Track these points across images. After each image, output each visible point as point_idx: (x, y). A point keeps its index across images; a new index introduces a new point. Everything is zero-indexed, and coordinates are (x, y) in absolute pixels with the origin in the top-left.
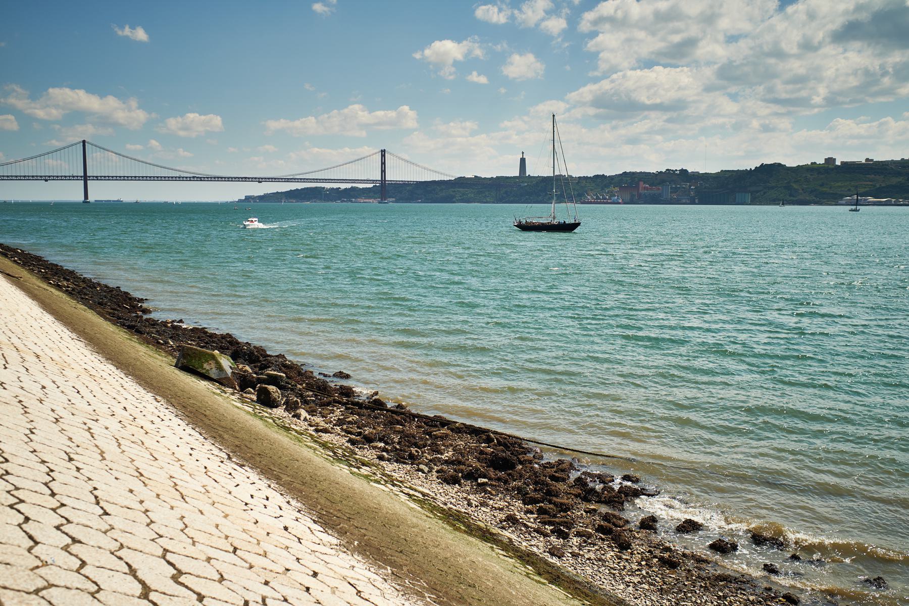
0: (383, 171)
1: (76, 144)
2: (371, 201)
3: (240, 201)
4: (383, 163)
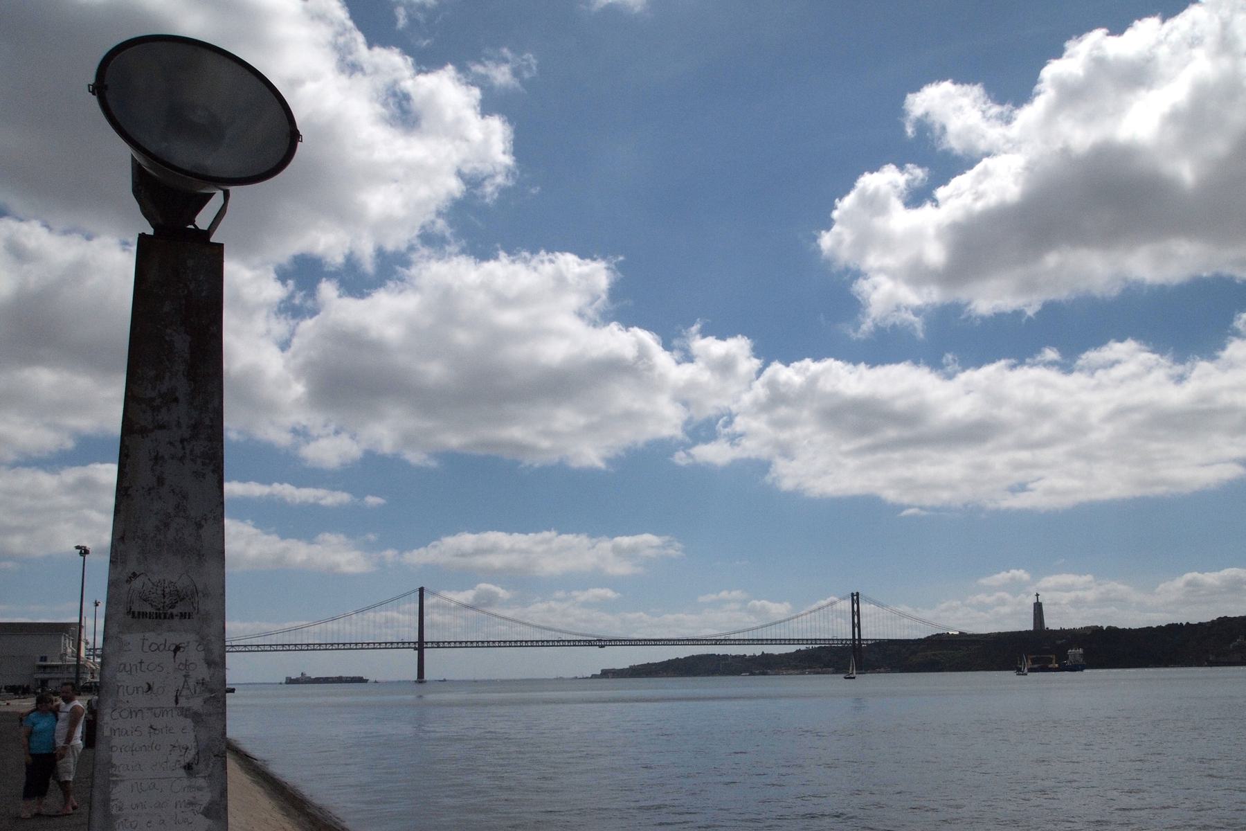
0: (856, 625)
1: (410, 593)
4: (856, 614)
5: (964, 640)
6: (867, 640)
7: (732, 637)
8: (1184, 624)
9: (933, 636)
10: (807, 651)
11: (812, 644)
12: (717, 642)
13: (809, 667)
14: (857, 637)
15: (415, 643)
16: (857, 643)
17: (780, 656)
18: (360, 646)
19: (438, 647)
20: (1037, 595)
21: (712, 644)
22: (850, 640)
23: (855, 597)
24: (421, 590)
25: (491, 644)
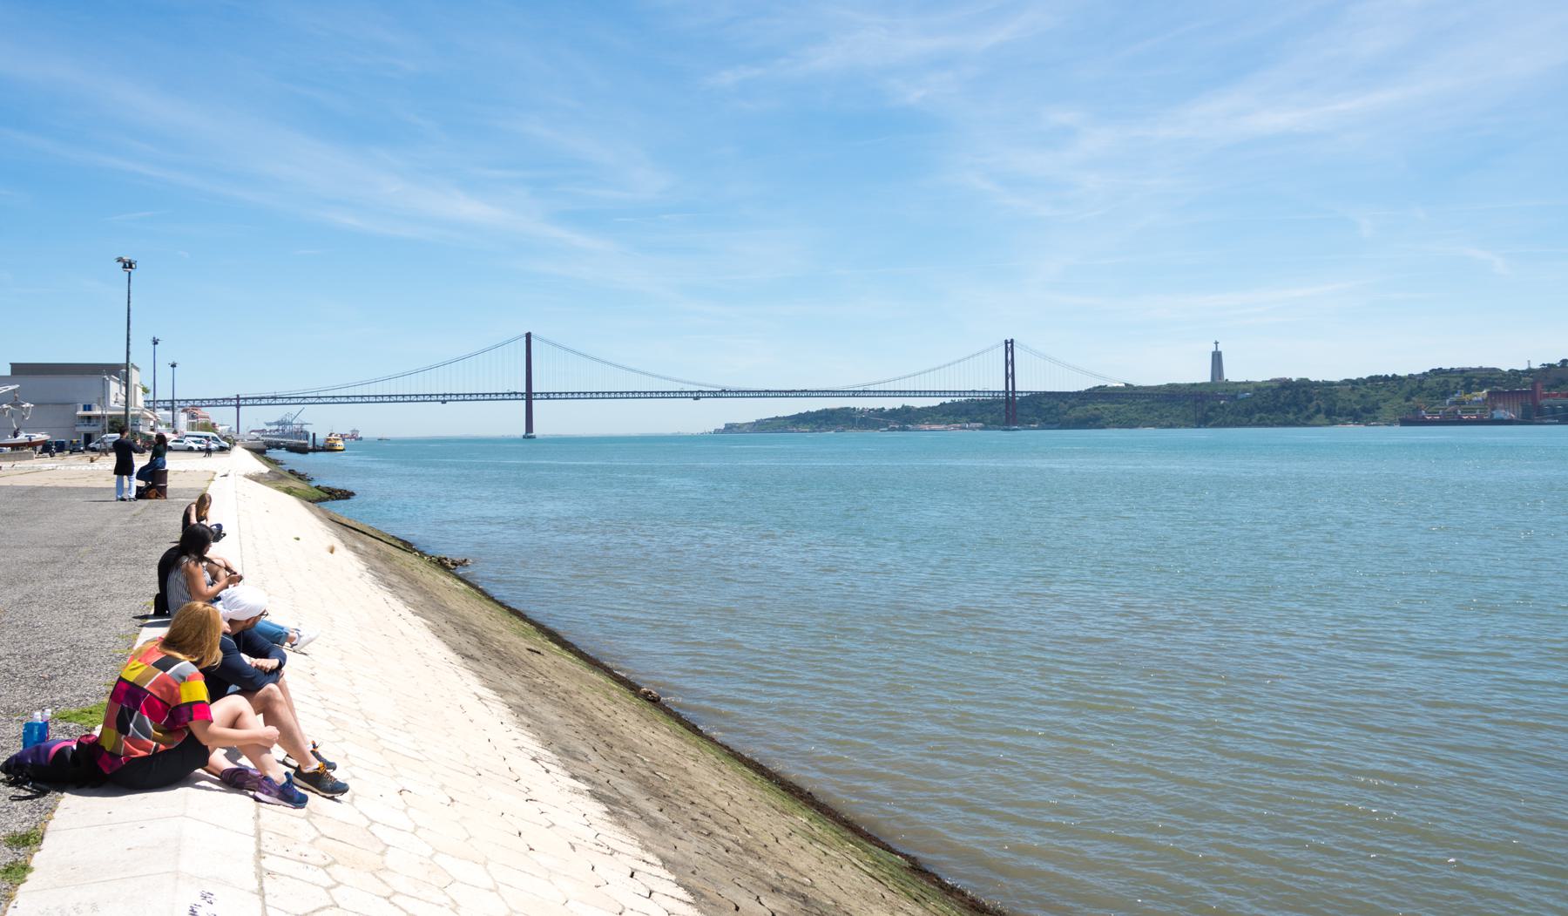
0: (1010, 376)
2: (942, 427)
3: (717, 431)
4: (1010, 363)
5: (1129, 395)
6: (1022, 392)
7: (871, 388)
8: (1390, 376)
9: (1095, 388)
10: (953, 403)
11: (960, 396)
12: (855, 394)
13: (955, 422)
14: (1010, 389)
15: (522, 394)
16: (1010, 395)
17: (922, 409)
18: (461, 397)
19: (548, 398)
20: (1216, 343)
21: (849, 396)
22: (1003, 392)
23: (1009, 345)
24: (528, 336)
25: (607, 395)
